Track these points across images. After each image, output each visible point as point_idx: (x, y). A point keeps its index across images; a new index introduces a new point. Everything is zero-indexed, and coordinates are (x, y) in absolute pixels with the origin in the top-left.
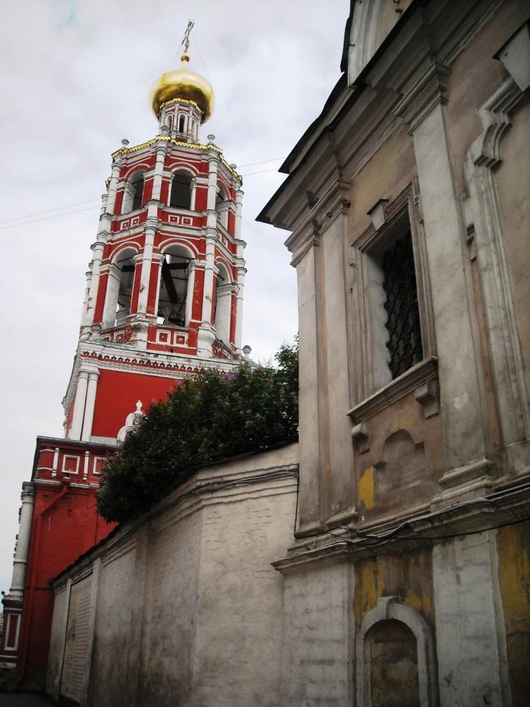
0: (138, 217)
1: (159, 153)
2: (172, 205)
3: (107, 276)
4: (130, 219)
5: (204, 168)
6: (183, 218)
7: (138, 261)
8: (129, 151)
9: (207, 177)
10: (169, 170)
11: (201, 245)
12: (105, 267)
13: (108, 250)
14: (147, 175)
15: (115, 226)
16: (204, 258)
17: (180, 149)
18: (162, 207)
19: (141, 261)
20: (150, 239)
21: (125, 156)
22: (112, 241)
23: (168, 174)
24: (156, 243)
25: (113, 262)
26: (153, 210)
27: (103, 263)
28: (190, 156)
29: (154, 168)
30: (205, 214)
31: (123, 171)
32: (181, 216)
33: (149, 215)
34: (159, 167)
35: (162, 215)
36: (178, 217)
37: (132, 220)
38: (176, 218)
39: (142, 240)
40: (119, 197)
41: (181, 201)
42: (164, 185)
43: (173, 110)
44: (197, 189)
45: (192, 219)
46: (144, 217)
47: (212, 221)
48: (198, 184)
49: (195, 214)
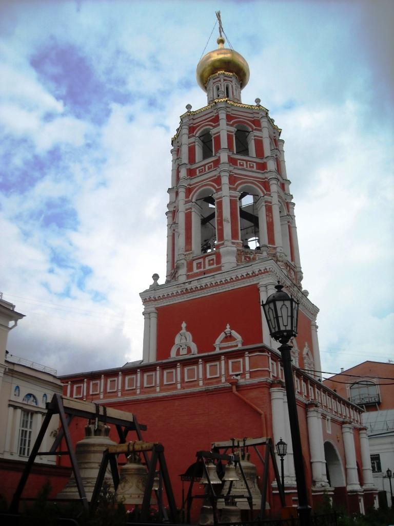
0: (212, 164)
1: (220, 112)
2: (238, 153)
3: (191, 212)
4: (204, 165)
5: (257, 123)
6: (248, 163)
8: (195, 113)
9: (260, 131)
10: (232, 125)
13: (189, 191)
15: (191, 173)
16: (270, 195)
17: (236, 109)
18: (230, 154)
19: (221, 198)
20: (225, 180)
21: (192, 117)
22: (190, 185)
25: (193, 201)
26: (224, 157)
27: (186, 202)
28: (246, 115)
29: (219, 125)
30: (265, 160)
31: (192, 130)
32: (247, 161)
33: (222, 161)
34: (223, 122)
35: (232, 161)
36: (245, 163)
37: (207, 166)
39: (218, 181)
40: (192, 151)
41: (243, 149)
42: (229, 138)
43: (220, 81)
44: (255, 139)
45: (255, 164)
46: (217, 163)
47: (271, 165)
48: (255, 136)
49: (258, 160)
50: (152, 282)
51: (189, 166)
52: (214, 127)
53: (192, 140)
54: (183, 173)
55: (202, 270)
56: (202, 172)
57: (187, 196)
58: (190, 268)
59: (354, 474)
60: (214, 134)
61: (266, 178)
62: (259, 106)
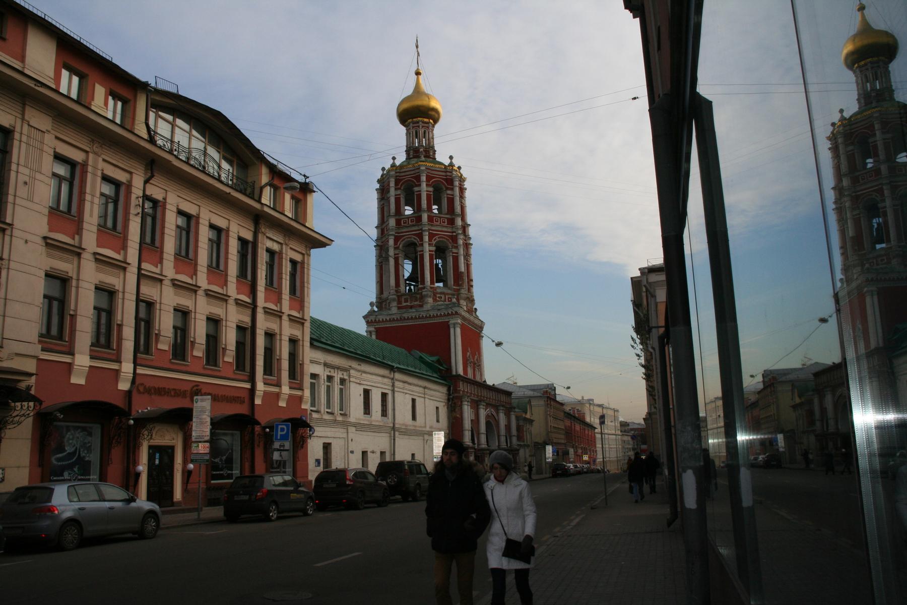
5: (450, 181)
11: (454, 239)
12: (397, 252)
13: (397, 240)
14: (416, 189)
15: (398, 222)
16: (457, 247)
20: (426, 238)
23: (431, 189)
24: (430, 240)
26: (425, 217)
34: (424, 185)
35: (430, 219)
39: (420, 236)
40: (397, 200)
42: (428, 196)
46: (419, 219)
47: (459, 222)
50: (369, 308)
52: (417, 186)
53: (399, 192)
54: (392, 222)
55: (408, 304)
57: (396, 243)
58: (399, 302)
59: (503, 439)
62: (451, 165)
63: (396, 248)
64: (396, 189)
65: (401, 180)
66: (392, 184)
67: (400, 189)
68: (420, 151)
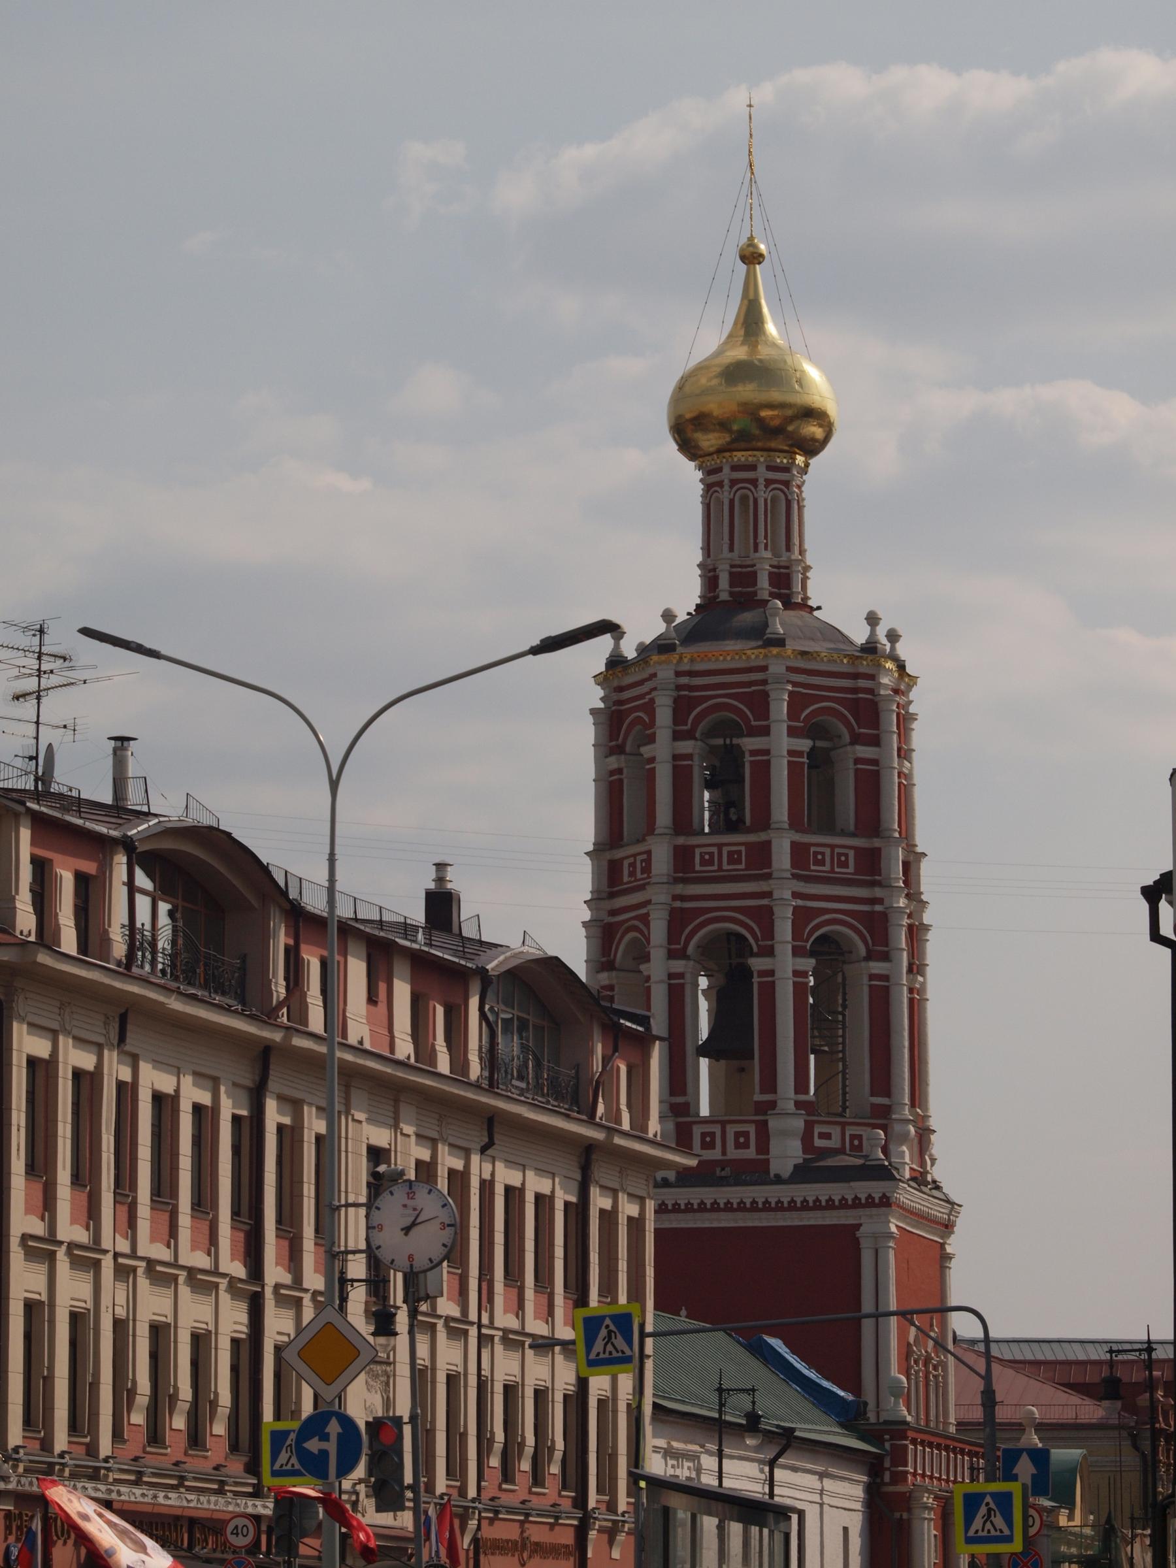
0: (743, 848)
6: (837, 850)
7: (762, 973)
12: (678, 966)
13: (678, 921)
14: (749, 743)
22: (682, 898)
31: (681, 708)
32: (832, 847)
36: (828, 851)
37: (725, 850)
38: (823, 854)
39: (765, 918)
45: (851, 853)
46: (761, 855)
48: (857, 761)
51: (681, 840)
53: (686, 747)
56: (710, 862)
60: (754, 753)
61: (880, 901)
63: (672, 955)
64: (677, 736)
65: (692, 703)
66: (664, 716)
67: (689, 735)
68: (750, 573)
